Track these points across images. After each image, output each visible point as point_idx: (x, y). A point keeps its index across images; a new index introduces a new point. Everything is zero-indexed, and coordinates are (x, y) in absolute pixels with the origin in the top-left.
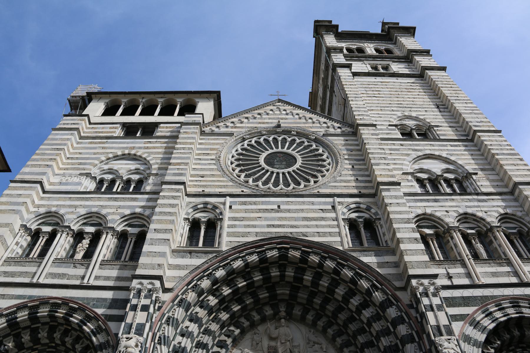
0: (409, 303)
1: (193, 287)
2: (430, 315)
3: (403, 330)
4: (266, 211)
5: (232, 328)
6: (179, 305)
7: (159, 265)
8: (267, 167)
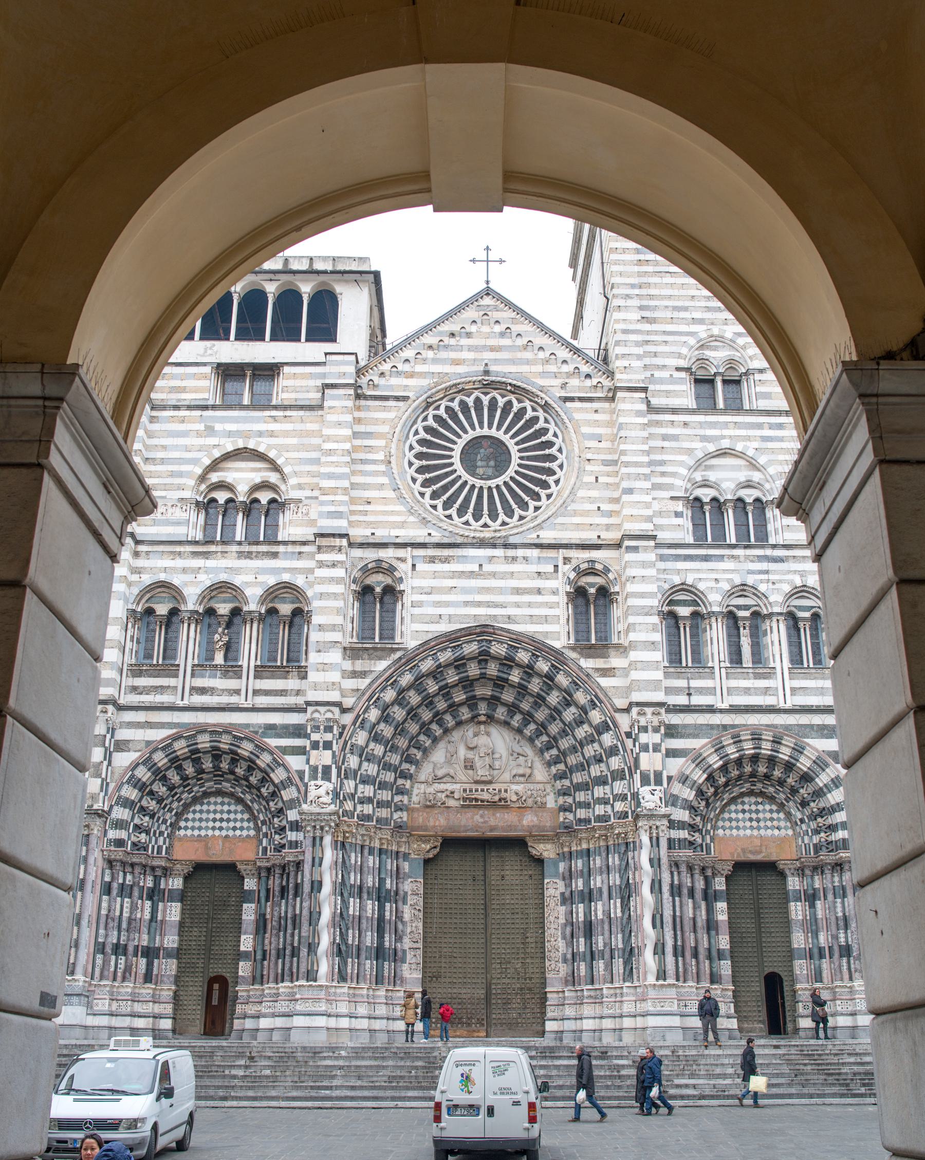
0: (629, 730)
1: (375, 701)
2: (644, 756)
3: (615, 763)
4: (462, 574)
5: (422, 738)
6: (362, 727)
7: (333, 684)
8: (466, 476)
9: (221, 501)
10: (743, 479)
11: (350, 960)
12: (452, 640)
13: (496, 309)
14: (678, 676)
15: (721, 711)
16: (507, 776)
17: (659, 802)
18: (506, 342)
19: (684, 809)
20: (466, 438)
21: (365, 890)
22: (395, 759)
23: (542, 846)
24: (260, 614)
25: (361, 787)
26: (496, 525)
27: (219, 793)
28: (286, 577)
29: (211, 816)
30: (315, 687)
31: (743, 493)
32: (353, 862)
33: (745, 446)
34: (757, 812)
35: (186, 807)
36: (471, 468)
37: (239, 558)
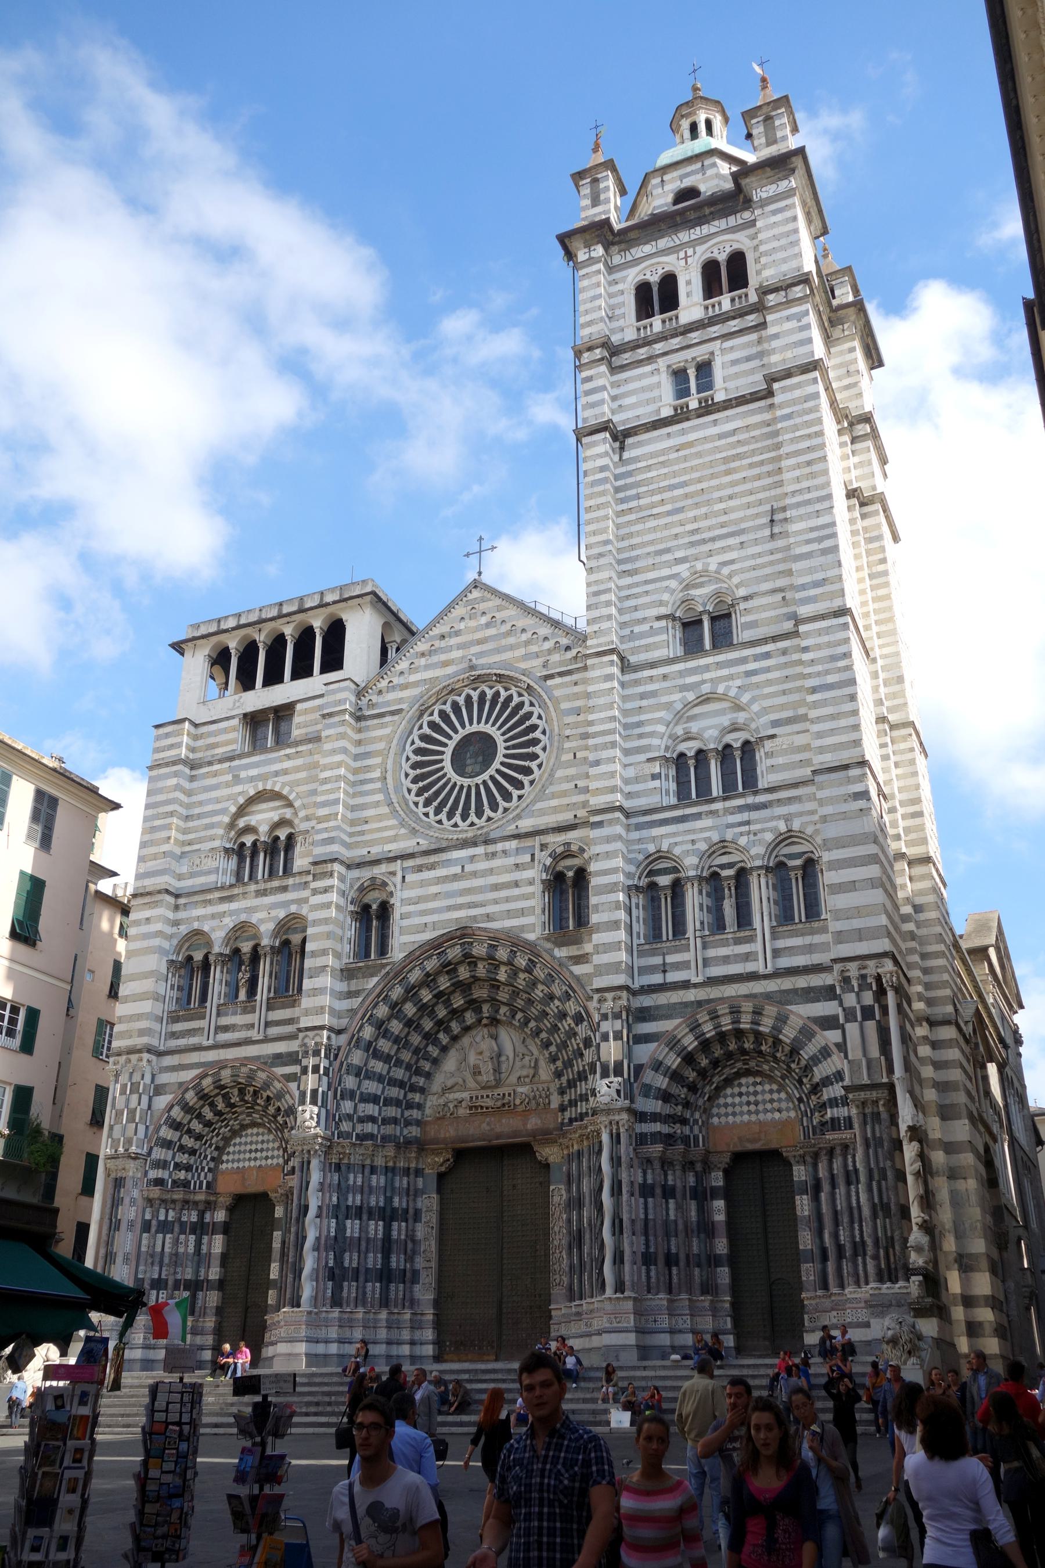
5: (430, 1048)
9: (248, 844)
10: (727, 723)
11: (346, 1284)
12: (436, 948)
13: (483, 600)
14: (653, 953)
15: (695, 986)
16: (513, 1079)
17: (616, 1096)
18: (492, 631)
19: (657, 1099)
20: (457, 738)
21: (364, 1211)
22: (399, 1073)
23: (547, 1150)
24: (272, 947)
25: (361, 1106)
26: (481, 822)
27: (253, 1124)
28: (293, 908)
29: (248, 1147)
30: (307, 1013)
31: (729, 739)
32: (351, 1182)
33: (728, 688)
34: (755, 1093)
35: (227, 1141)
36: (460, 771)
37: (257, 896)
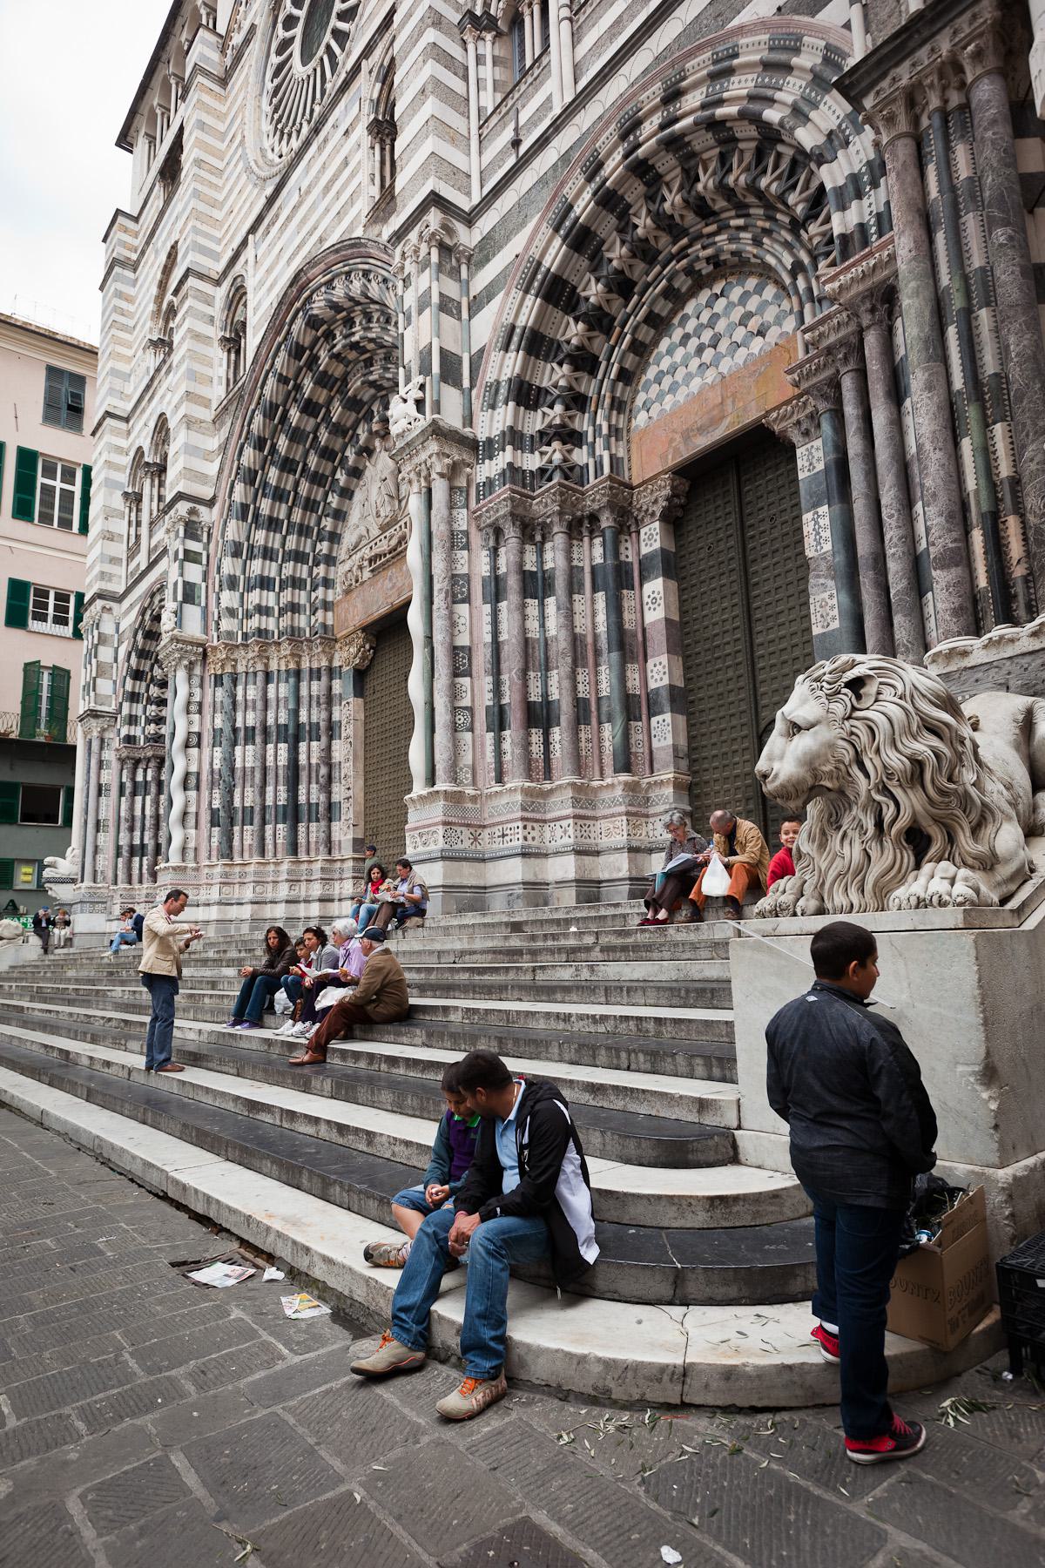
12: (278, 334)
32: (240, 697)
